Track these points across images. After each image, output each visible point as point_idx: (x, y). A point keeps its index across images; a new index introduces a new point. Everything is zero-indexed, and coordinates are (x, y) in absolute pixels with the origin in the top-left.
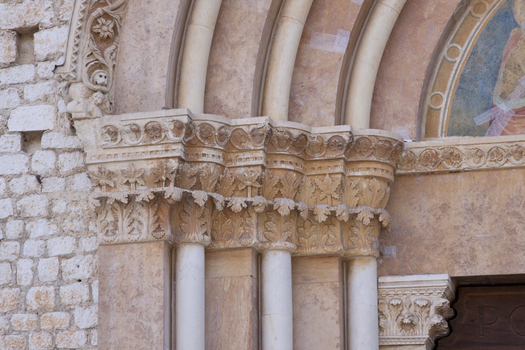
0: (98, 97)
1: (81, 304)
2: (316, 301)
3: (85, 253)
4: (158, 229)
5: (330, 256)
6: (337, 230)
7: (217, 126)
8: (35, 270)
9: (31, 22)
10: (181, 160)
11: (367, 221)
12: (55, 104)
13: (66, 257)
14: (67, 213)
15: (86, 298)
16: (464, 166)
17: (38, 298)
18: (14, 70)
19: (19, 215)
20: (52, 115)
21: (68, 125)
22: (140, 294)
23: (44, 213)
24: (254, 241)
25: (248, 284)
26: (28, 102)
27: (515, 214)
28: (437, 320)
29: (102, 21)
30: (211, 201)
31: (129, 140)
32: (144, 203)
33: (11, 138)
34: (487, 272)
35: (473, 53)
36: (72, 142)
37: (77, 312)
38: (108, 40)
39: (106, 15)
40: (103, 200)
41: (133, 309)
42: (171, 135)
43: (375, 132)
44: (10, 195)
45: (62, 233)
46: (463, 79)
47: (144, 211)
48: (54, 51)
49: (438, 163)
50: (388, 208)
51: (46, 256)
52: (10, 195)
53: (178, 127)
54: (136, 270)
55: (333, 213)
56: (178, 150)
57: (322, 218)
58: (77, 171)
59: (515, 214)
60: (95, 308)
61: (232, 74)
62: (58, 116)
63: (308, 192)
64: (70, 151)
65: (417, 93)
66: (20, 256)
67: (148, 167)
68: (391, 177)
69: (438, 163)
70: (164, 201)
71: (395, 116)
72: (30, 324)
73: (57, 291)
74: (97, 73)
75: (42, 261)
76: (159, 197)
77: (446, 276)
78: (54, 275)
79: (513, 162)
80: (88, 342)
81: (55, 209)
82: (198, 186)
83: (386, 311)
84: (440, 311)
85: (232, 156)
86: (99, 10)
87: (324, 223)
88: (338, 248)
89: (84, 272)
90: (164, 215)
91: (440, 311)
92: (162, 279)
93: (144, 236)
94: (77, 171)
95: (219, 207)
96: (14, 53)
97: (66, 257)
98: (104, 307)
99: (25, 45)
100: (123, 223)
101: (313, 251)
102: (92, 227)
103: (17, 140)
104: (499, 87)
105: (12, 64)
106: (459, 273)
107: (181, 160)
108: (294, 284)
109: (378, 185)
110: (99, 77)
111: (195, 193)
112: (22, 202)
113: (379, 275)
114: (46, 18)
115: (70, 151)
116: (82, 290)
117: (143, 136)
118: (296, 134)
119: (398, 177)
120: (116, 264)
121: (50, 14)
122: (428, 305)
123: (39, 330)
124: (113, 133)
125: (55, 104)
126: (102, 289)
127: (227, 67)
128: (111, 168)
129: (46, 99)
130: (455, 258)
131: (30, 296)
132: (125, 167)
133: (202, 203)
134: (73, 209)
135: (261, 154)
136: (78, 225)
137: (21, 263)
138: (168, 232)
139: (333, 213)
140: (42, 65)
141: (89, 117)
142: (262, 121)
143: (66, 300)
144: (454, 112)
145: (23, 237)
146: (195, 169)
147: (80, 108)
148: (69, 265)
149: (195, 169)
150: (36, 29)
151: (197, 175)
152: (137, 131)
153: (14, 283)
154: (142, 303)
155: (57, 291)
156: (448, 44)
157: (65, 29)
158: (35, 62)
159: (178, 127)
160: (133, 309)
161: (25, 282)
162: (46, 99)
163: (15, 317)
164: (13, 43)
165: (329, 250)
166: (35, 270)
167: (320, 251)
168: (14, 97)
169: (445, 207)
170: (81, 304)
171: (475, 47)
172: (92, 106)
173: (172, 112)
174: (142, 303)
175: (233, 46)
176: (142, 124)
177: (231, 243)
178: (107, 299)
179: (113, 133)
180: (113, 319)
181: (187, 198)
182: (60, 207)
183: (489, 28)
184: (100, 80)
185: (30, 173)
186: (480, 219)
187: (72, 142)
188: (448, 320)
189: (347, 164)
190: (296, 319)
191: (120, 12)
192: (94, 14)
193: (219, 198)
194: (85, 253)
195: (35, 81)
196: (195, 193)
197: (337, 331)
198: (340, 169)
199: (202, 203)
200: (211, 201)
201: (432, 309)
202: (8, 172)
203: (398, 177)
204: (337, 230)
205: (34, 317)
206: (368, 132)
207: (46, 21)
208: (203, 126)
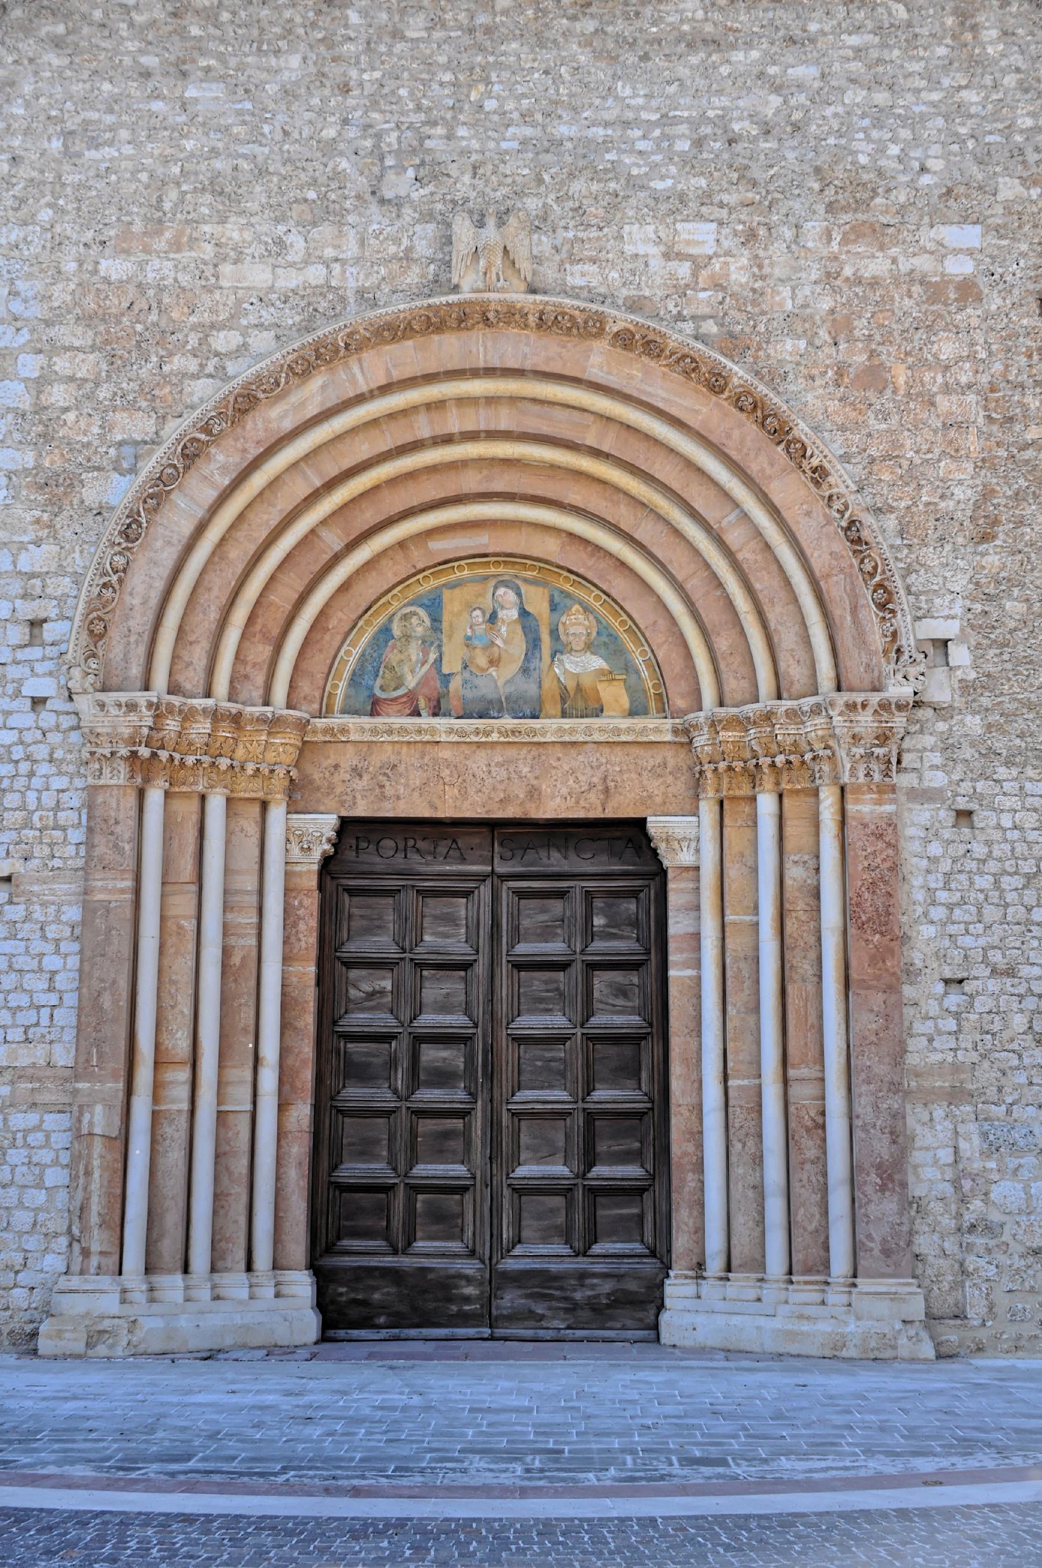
0: (91, 678)
1: (73, 826)
2: (242, 830)
3: (77, 789)
4: (132, 777)
5: (254, 799)
6: (260, 781)
7: (177, 704)
8: (39, 799)
9: (42, 615)
10: (151, 729)
11: (282, 775)
12: (57, 678)
13: (63, 791)
14: (63, 760)
15: (76, 821)
16: (352, 738)
17: (41, 819)
18: (27, 650)
19: (27, 758)
20: (55, 686)
21: (67, 694)
22: (117, 823)
23: (47, 757)
24: (200, 788)
25: (195, 818)
26: (37, 675)
27: (385, 774)
28: (327, 847)
29: (96, 622)
30: (172, 759)
31: (114, 711)
32: (122, 757)
33: (24, 700)
34: (363, 814)
35: (363, 655)
36: (68, 707)
37: (69, 831)
38: (101, 636)
39: (100, 619)
40: (92, 753)
41: (112, 833)
42: (144, 709)
43: (291, 712)
44: (22, 743)
45: (60, 773)
46: (354, 673)
47: (122, 763)
48: (58, 638)
49: (333, 735)
50: (296, 766)
51: (47, 789)
52: (22, 743)
53: (150, 705)
54: (114, 805)
55: (258, 769)
56: (149, 722)
57: (250, 772)
58: (74, 728)
59: (385, 774)
60: (83, 830)
61: (189, 664)
62: (60, 687)
63: (240, 753)
64: (68, 713)
65: (321, 683)
66: (28, 788)
67: (127, 732)
68: (299, 744)
69: (333, 735)
70: (138, 757)
71: (305, 698)
72: (34, 838)
73: (55, 815)
74: (91, 661)
75: (45, 793)
76: (134, 754)
77: (335, 816)
78: (53, 804)
79: (386, 738)
80: (77, 853)
81: (55, 756)
82: (162, 747)
83: (292, 838)
84: (329, 840)
85: (187, 725)
86: (95, 614)
87: (253, 776)
88: (260, 795)
89: (76, 803)
90: (137, 768)
91: (329, 840)
92: (133, 813)
93: (121, 782)
94: (74, 728)
95: (176, 762)
96: (27, 637)
97: (63, 791)
98: (90, 830)
99: (36, 631)
100: (106, 771)
101: (242, 795)
102: (82, 771)
103: (28, 703)
104: (379, 682)
105: (26, 646)
106: (344, 814)
107: (151, 729)
108: (228, 816)
109: (291, 749)
110: (93, 664)
111: (160, 752)
112: (30, 748)
113: (288, 813)
114: (53, 613)
115: (68, 713)
116: (73, 816)
117: (124, 709)
118: (234, 711)
119: (304, 743)
120: (100, 800)
121: (56, 611)
122: (322, 835)
123: (41, 843)
124: (102, 706)
125: (57, 678)
126: (90, 818)
127: (186, 659)
128: (99, 730)
129: (51, 674)
130: (342, 803)
131: (36, 817)
132: (109, 730)
133: (164, 760)
134: (69, 756)
135: (208, 725)
136: (71, 768)
137: (29, 793)
138: (139, 780)
139: (258, 769)
140: (48, 648)
141: (85, 692)
142: (210, 702)
143: (61, 822)
144: (347, 697)
145: (31, 774)
146: (161, 734)
147: (78, 685)
148: (64, 797)
149: (161, 734)
150: (45, 621)
151: (162, 739)
152: (120, 706)
153: (23, 807)
154: (118, 829)
155: (55, 815)
156: (345, 648)
157: (68, 623)
158: (43, 645)
159: (150, 705)
160: (112, 833)
161: (32, 807)
162: (51, 674)
163: (24, 832)
164: (27, 630)
165: (253, 795)
166: (39, 799)
167: (247, 795)
168: (27, 670)
169: (336, 767)
170: (73, 826)
171: (364, 651)
172: (87, 685)
173: (146, 693)
174: (118, 829)
175: (191, 643)
176: (123, 700)
177: (184, 789)
178: (92, 824)
179: (102, 706)
180: (98, 839)
181: (154, 755)
182: (59, 754)
183: (375, 638)
184: (94, 666)
185: (38, 728)
186: (361, 776)
187: (68, 707)
188: (334, 845)
189: (269, 734)
190: (228, 842)
191: (110, 616)
192: (91, 616)
193: (177, 756)
194: (77, 789)
195: (43, 660)
196: (160, 752)
197: (256, 852)
198: (264, 737)
199: (164, 760)
200: (172, 759)
201: (324, 839)
202: (21, 726)
203: (304, 743)
204: (260, 781)
205: (37, 833)
206: (286, 712)
207: (53, 616)
208: (168, 704)
